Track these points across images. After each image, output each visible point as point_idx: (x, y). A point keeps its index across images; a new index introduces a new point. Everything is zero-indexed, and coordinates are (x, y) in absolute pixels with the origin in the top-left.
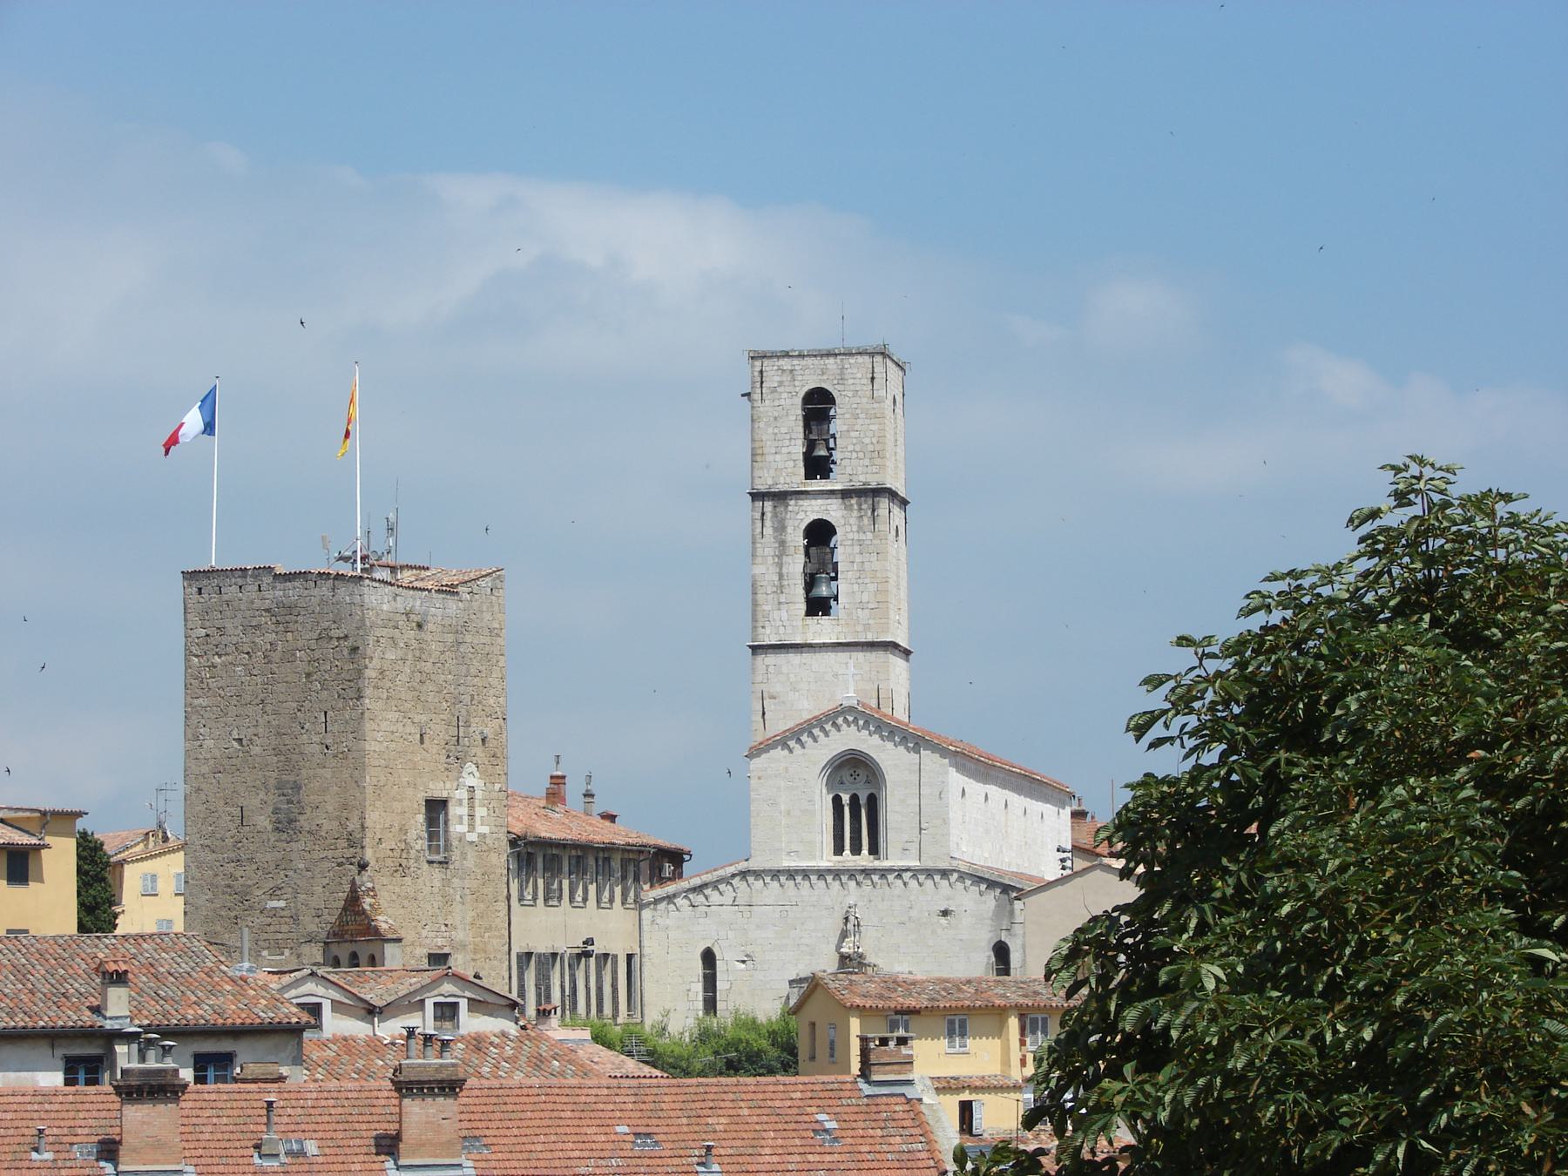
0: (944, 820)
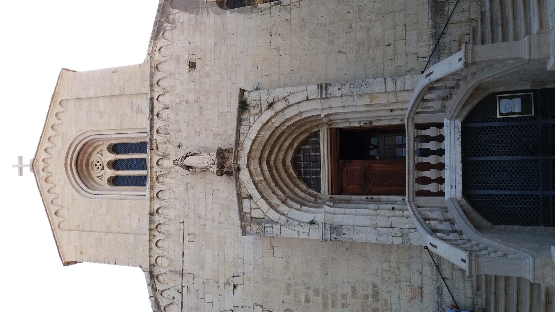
0: (113, 72)
